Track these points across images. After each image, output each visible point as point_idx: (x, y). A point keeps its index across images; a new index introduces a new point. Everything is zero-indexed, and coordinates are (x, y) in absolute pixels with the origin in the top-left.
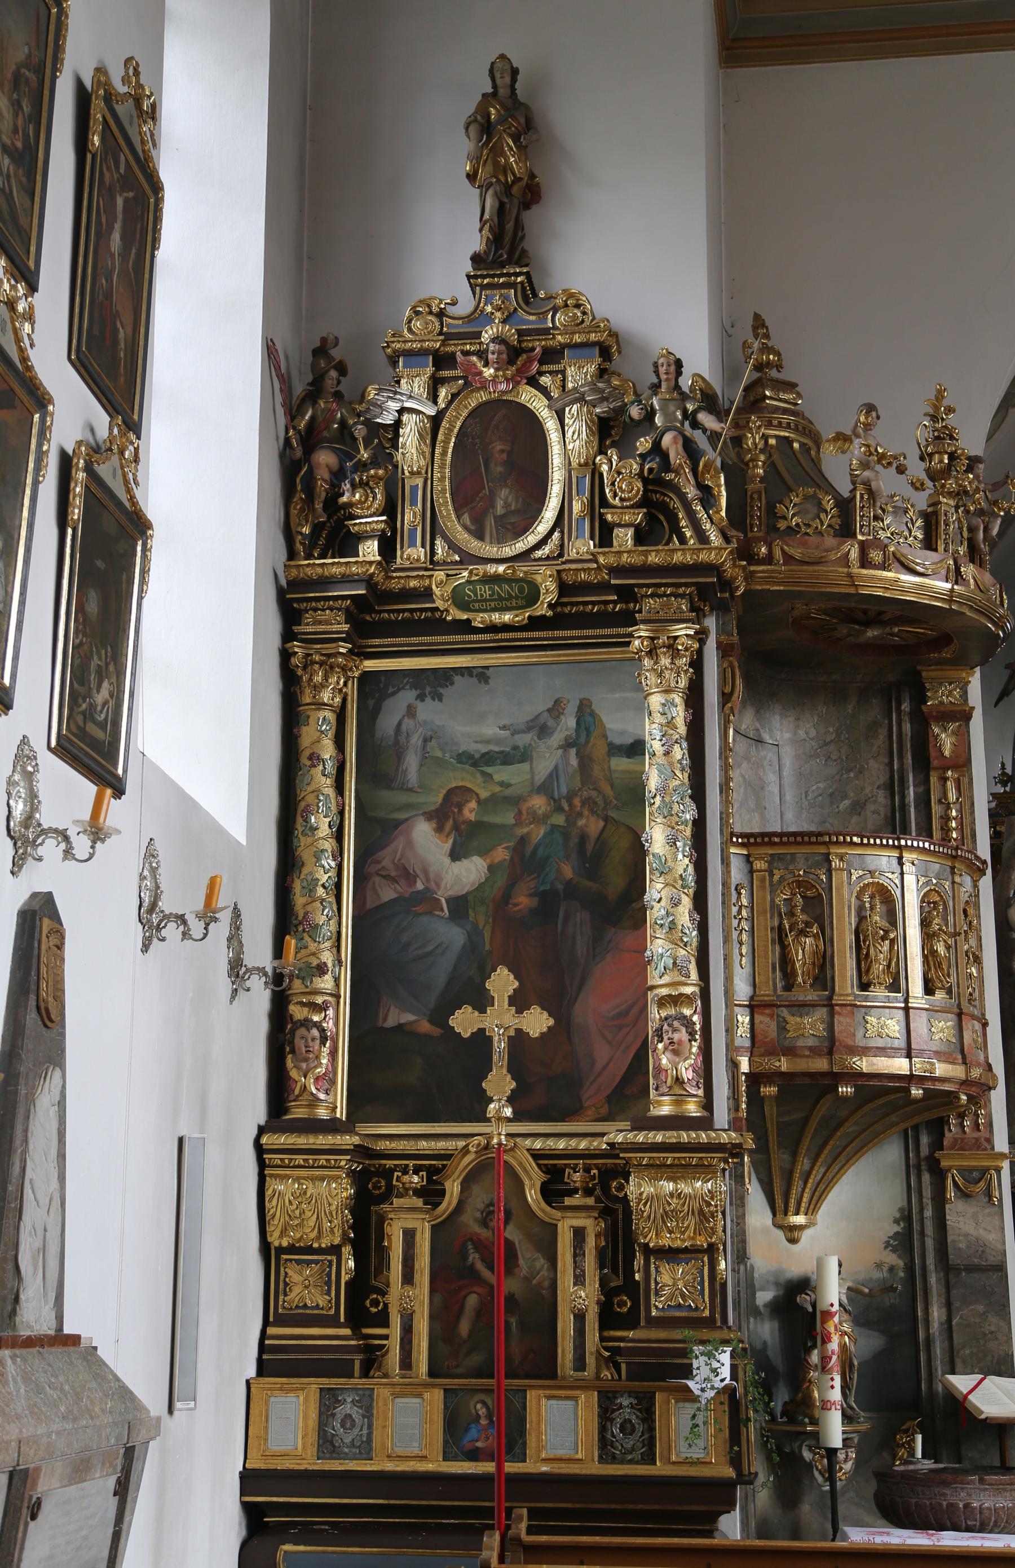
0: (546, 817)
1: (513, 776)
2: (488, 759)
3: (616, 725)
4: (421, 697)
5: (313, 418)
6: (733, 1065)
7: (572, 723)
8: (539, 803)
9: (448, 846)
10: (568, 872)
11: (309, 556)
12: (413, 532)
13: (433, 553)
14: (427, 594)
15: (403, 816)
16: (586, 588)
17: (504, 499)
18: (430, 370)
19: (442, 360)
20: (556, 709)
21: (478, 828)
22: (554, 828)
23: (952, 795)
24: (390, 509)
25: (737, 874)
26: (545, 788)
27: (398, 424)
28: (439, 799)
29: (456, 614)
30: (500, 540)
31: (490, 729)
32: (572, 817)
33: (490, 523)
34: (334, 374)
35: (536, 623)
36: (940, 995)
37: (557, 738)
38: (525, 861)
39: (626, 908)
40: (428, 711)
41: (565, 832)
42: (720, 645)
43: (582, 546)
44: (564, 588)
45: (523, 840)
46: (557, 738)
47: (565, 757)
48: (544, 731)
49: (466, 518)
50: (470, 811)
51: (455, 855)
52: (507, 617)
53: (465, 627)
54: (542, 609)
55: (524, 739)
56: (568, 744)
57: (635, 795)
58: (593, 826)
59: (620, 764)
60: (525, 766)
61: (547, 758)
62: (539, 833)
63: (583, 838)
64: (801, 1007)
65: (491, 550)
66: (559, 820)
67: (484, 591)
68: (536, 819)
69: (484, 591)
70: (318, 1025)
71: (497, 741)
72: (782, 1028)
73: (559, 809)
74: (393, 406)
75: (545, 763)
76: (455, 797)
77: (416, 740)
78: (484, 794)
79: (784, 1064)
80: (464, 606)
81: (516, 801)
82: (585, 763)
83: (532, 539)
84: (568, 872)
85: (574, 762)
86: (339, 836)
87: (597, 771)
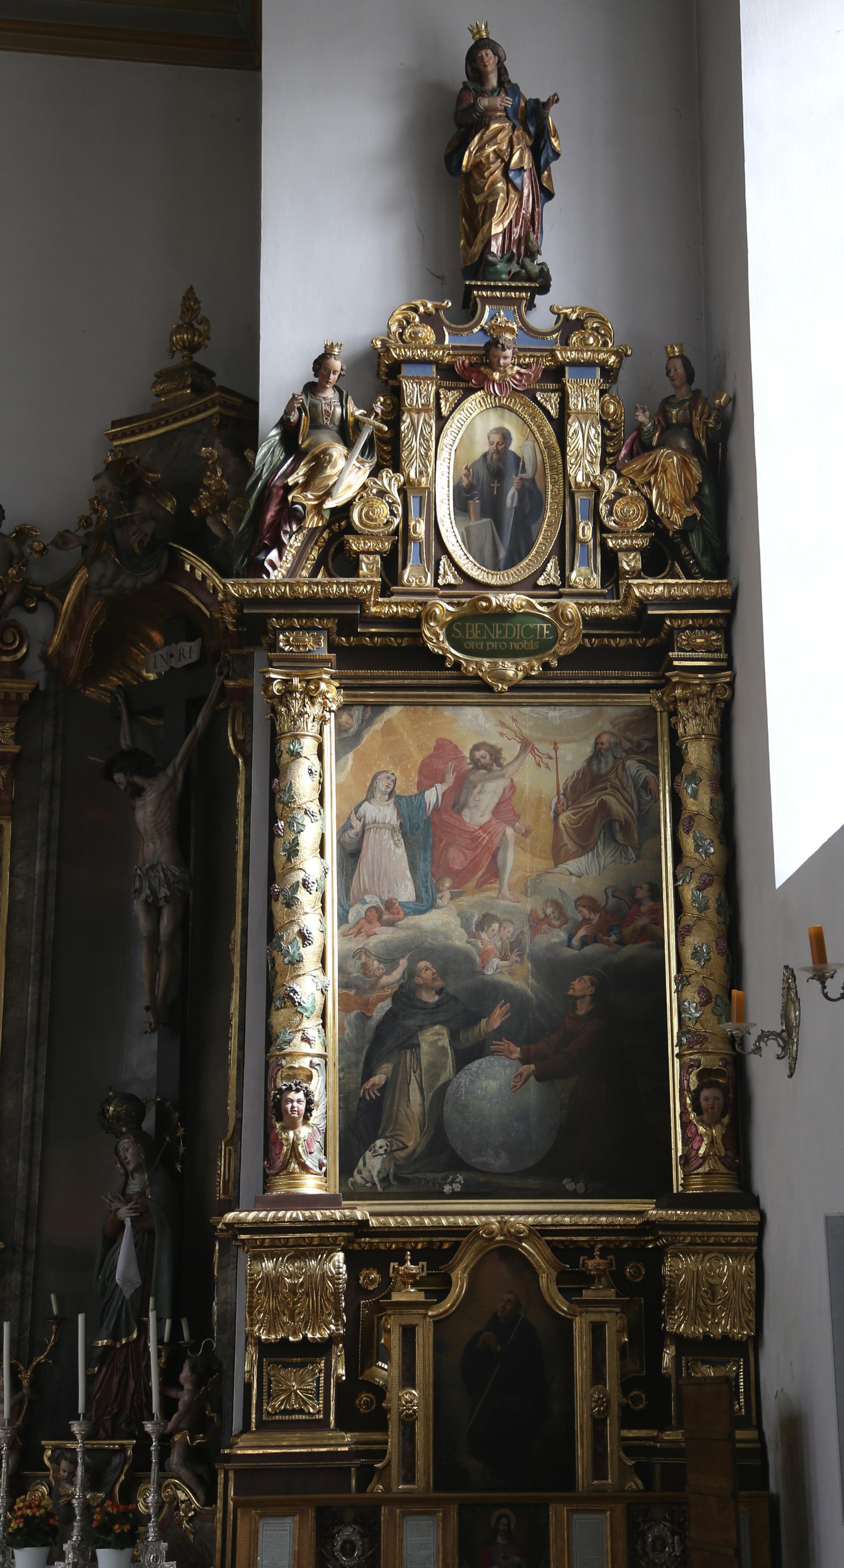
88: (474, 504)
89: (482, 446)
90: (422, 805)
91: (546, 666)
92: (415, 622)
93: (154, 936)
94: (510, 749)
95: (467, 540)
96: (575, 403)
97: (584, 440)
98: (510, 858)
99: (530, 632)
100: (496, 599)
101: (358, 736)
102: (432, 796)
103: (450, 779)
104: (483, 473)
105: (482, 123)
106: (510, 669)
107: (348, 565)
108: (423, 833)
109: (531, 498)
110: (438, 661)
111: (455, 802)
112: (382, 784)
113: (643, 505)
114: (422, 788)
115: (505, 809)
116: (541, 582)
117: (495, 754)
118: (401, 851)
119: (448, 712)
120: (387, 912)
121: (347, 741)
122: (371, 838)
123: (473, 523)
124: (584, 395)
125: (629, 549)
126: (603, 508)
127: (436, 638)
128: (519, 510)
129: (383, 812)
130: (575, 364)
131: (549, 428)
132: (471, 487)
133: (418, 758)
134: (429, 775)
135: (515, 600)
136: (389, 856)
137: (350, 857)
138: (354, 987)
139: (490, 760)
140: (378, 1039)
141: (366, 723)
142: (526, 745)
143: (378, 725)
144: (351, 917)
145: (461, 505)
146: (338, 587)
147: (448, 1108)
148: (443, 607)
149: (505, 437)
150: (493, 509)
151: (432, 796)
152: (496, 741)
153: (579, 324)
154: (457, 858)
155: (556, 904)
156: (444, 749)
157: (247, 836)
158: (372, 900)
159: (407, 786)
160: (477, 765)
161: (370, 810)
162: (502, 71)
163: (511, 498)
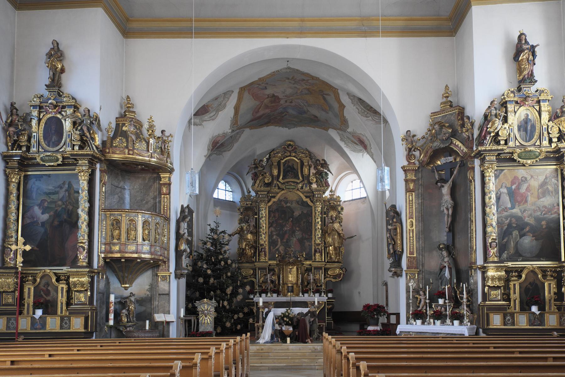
0: (61, 206)
1: (55, 197)
2: (50, 193)
3: (75, 186)
4: (36, 180)
5: (12, 120)
6: (99, 256)
7: (67, 186)
8: (60, 203)
9: (41, 211)
10: (65, 217)
11: (12, 150)
12: (34, 145)
13: (38, 149)
14: (35, 159)
15: (31, 205)
16: (68, 158)
17: (54, 138)
18: (38, 109)
19: (41, 107)
20: (64, 183)
21: (48, 207)
22: (63, 208)
23: (166, 200)
24: (29, 140)
25: (103, 218)
26: (61, 200)
27: (31, 121)
28: (39, 202)
29: (42, 163)
30: (53, 147)
31: (50, 187)
32: (66, 206)
33: (51, 143)
34: (15, 110)
35: (59, 165)
36: (147, 242)
37: (64, 189)
38: (57, 215)
39: (74, 225)
40: (38, 183)
41: (65, 209)
42: (100, 170)
43: (69, 149)
44: (64, 158)
45: (57, 210)
46: (64, 189)
47: (65, 193)
48: (61, 188)
49: (46, 142)
50: (46, 204)
51: (43, 213)
52: (52, 164)
53: (44, 165)
54: (60, 162)
55: (58, 189)
56: (66, 191)
57: (77, 201)
58: (70, 207)
59: (76, 195)
60: (57, 195)
61: (62, 193)
62: (60, 209)
63: (68, 210)
64: (115, 244)
65: (51, 149)
66: (64, 206)
67: (47, 158)
68: (59, 206)
69: (47, 158)
70: (10, 248)
71: (52, 190)
72: (111, 248)
73: (64, 204)
74: (30, 118)
75: (61, 195)
76: (43, 201)
77: (35, 189)
78: (49, 201)
79: (110, 255)
80: (44, 161)
81: (55, 202)
82: (69, 194)
83: (59, 147)
84: (65, 217)
85: (67, 194)
86: (18, 209)
87: (72, 196)
88: (522, 129)
89: (523, 117)
90: (512, 189)
91: (537, 161)
92: (512, 153)
93: (448, 214)
94: (529, 178)
95: (520, 137)
96: (543, 109)
97: (545, 116)
98: (529, 199)
99: (535, 154)
100: (529, 149)
101: (499, 176)
102: (514, 187)
103: (517, 183)
104: (523, 123)
105: (523, 51)
106: (529, 162)
107: (498, 143)
108: (512, 194)
109: (533, 127)
110: (514, 161)
111: (518, 188)
112: (504, 185)
113: (558, 128)
114: (512, 185)
115: (528, 189)
116: (536, 144)
117: (526, 178)
118: (508, 198)
119: (516, 171)
120: (506, 209)
121: (496, 177)
122: (502, 195)
123: (522, 133)
124: (545, 107)
125: (554, 137)
126: (549, 130)
127: (515, 157)
128: (531, 130)
129: (504, 190)
130: (543, 100)
131: (537, 113)
132: (521, 126)
133: (511, 180)
134: (513, 183)
135: (532, 148)
136: (506, 199)
137: (498, 198)
138: (499, 223)
139: (525, 180)
140: (505, 232)
141: (500, 173)
142: (532, 177)
143: (502, 174)
144: (499, 210)
145: (519, 130)
146: (495, 147)
147: (518, 246)
148: (518, 151)
149: (527, 115)
150: (526, 130)
151: (514, 187)
152: (526, 176)
153: (543, 91)
154: (519, 199)
155: (539, 208)
156: (516, 178)
157: (475, 195)
158: (503, 207)
159: (509, 185)
160: (522, 181)
161: (502, 190)
162: (526, 39)
163: (529, 128)
